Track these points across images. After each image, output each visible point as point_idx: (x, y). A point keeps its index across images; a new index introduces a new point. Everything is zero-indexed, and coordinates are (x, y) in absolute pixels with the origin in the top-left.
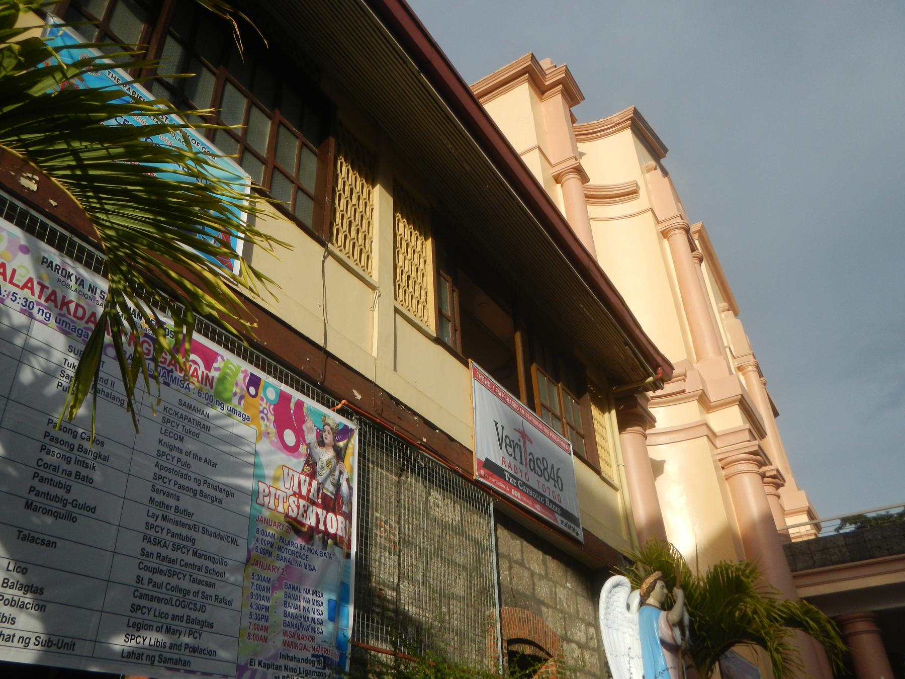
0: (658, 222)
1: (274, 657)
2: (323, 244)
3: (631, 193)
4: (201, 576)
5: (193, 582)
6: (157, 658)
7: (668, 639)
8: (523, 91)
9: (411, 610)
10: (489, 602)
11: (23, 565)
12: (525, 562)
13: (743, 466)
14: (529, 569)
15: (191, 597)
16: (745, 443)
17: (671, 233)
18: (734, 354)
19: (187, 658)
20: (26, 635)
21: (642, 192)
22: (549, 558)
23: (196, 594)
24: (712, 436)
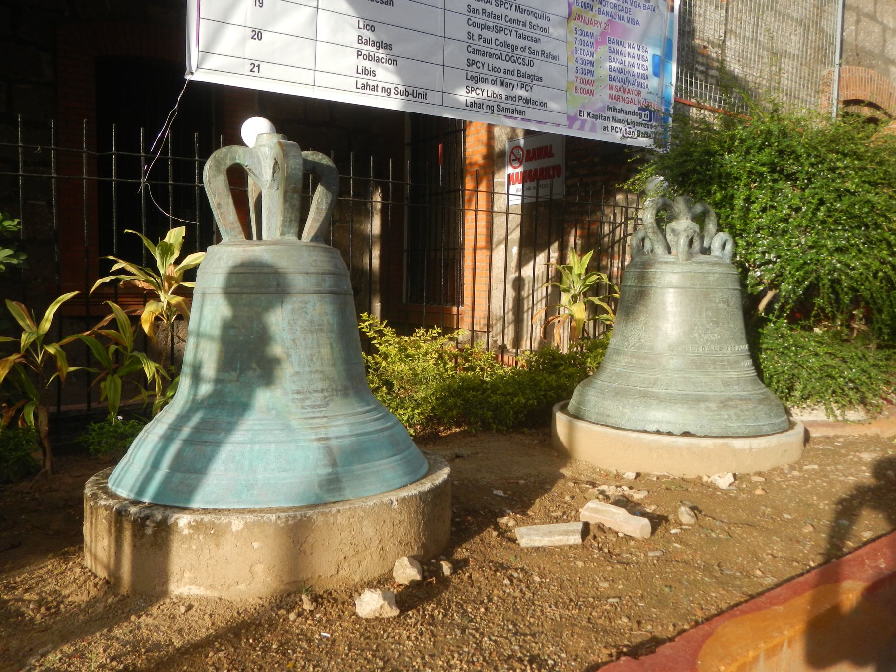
1: (602, 109)
4: (526, 31)
5: (519, 37)
6: (496, 108)
10: (824, 59)
11: (371, 23)
12: (878, 15)
14: (881, 23)
15: (519, 52)
19: (522, 109)
20: (387, 85)
23: (523, 49)
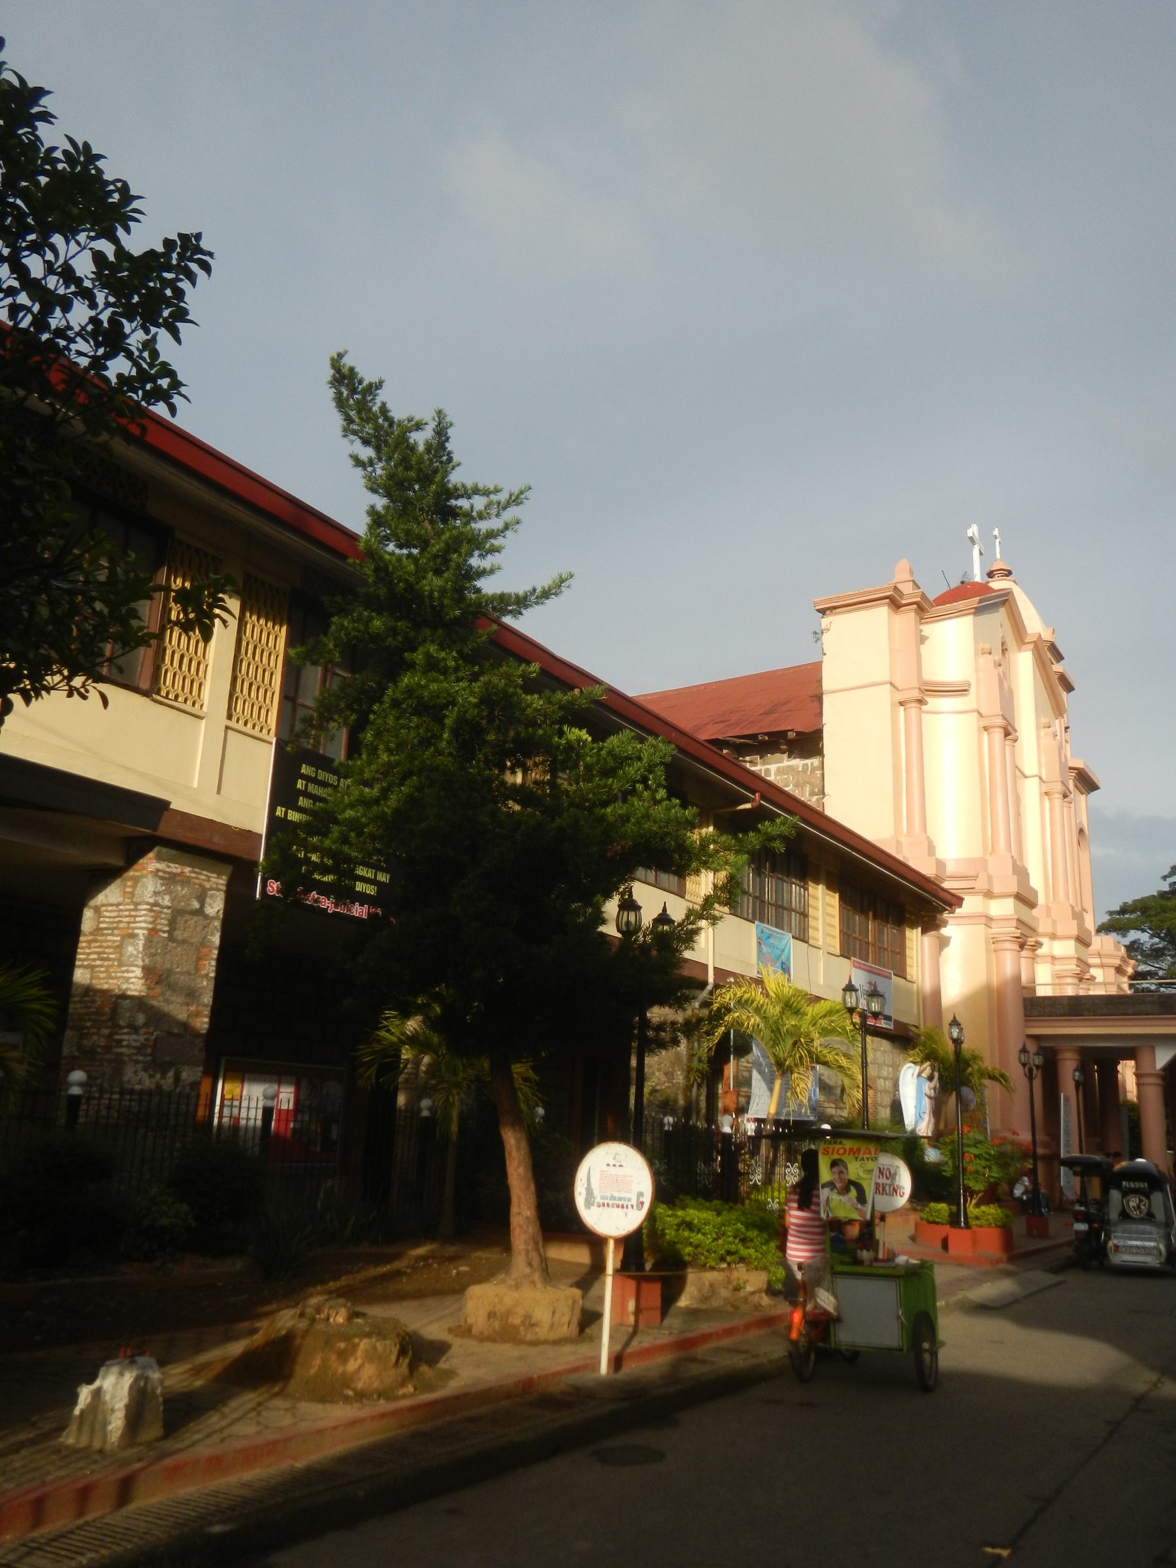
0: (981, 715)
2: (807, 942)
3: (961, 690)
7: (928, 1094)
8: (882, 612)
9: (828, 1081)
13: (1008, 945)
16: (1011, 929)
17: (991, 730)
18: (1044, 778)
21: (973, 690)
22: (874, 1038)
24: (988, 920)
